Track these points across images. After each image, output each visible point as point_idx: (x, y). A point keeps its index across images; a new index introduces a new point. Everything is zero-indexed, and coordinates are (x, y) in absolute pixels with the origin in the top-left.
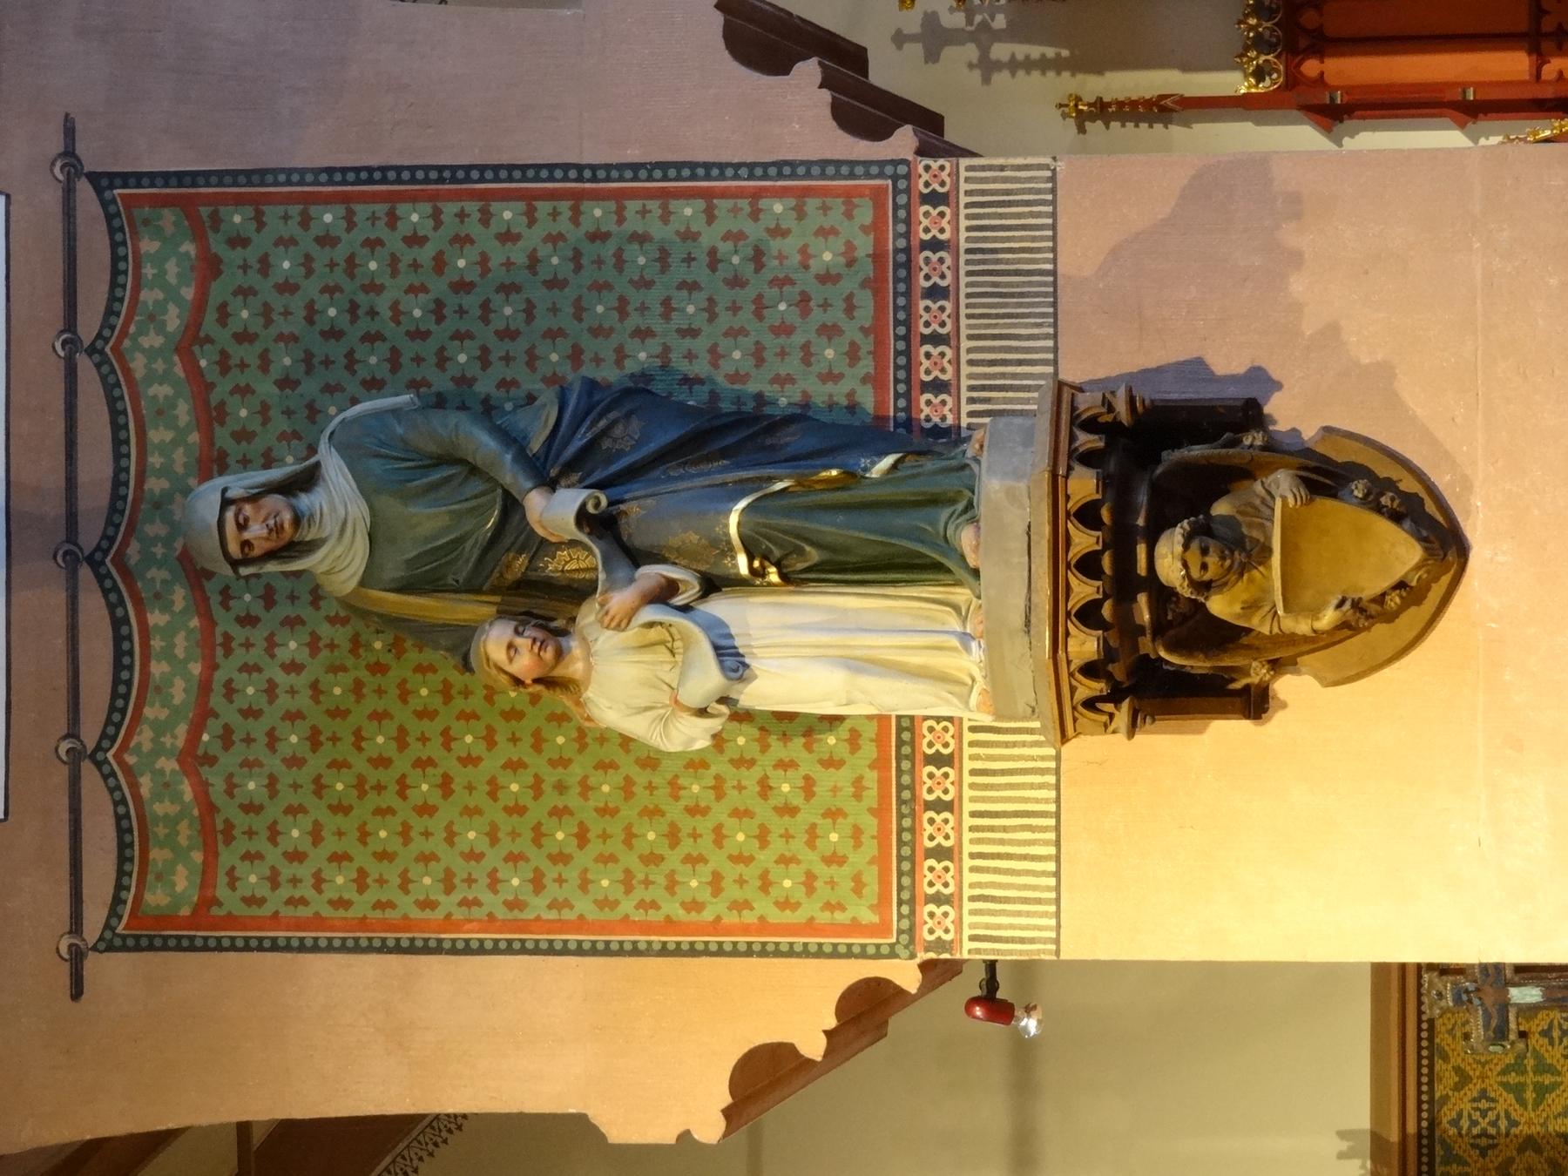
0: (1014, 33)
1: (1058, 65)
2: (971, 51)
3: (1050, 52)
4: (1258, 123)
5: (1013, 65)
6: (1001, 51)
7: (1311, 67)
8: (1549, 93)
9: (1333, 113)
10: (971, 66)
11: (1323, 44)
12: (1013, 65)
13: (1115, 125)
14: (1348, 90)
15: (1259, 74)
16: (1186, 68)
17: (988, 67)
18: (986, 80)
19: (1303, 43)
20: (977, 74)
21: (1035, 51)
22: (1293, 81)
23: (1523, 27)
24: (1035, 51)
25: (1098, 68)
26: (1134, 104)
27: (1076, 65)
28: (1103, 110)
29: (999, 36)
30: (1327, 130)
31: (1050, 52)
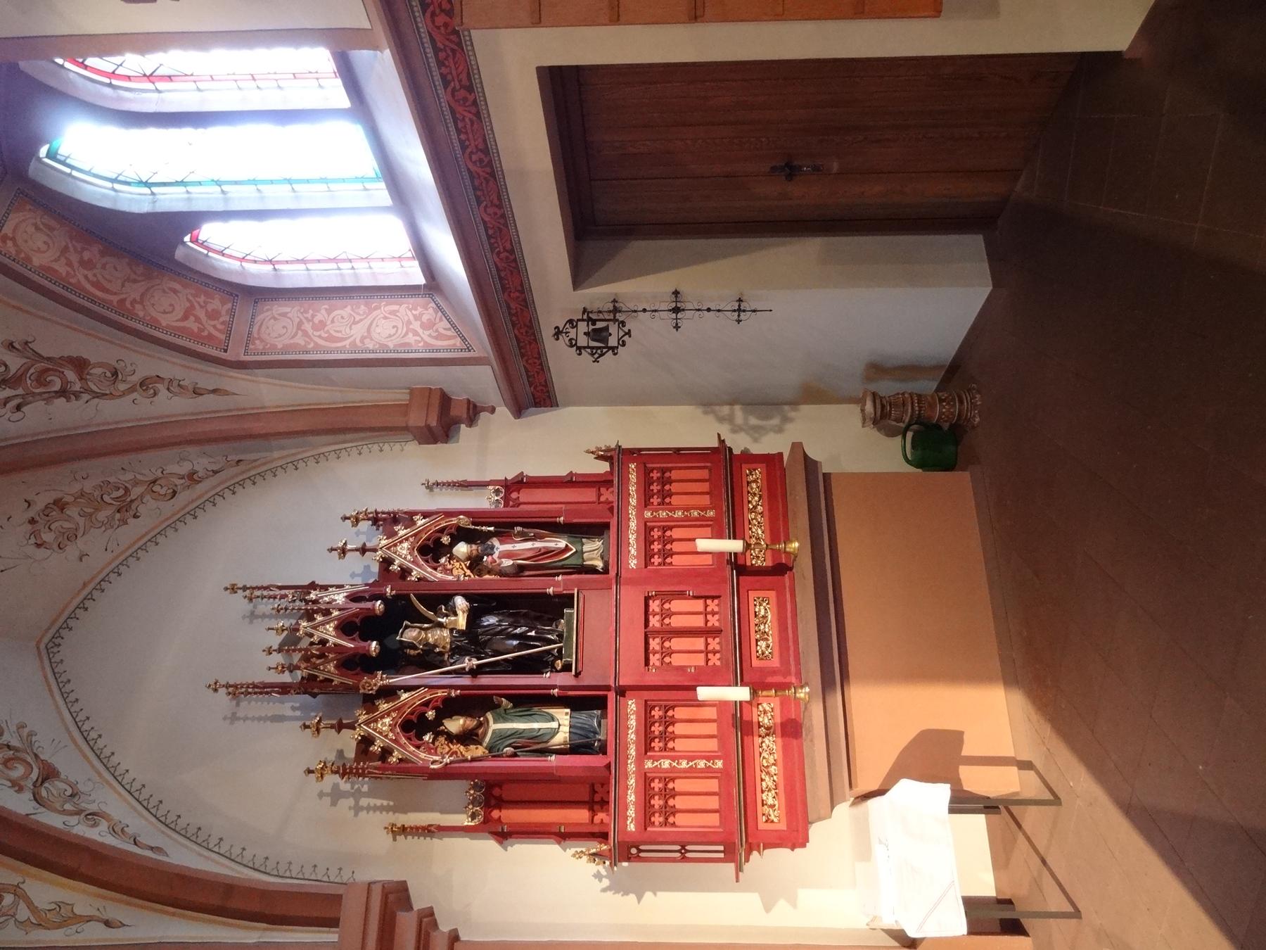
0: (370, 794)
1: (387, 809)
2: (351, 801)
3: (385, 803)
4: (472, 839)
5: (368, 809)
6: (364, 802)
7: (495, 814)
8: (596, 829)
9: (504, 835)
10: (350, 808)
11: (501, 803)
12: (368, 809)
13: (410, 837)
14: (510, 825)
15: (473, 816)
16: (442, 812)
17: (357, 809)
18: (356, 815)
19: (493, 802)
20: (352, 812)
21: (379, 802)
22: (487, 820)
23: (587, 799)
24: (379, 802)
25: (405, 811)
26: (417, 828)
27: (394, 809)
28: (404, 830)
29: (368, 795)
30: (501, 843)
31: (385, 803)
